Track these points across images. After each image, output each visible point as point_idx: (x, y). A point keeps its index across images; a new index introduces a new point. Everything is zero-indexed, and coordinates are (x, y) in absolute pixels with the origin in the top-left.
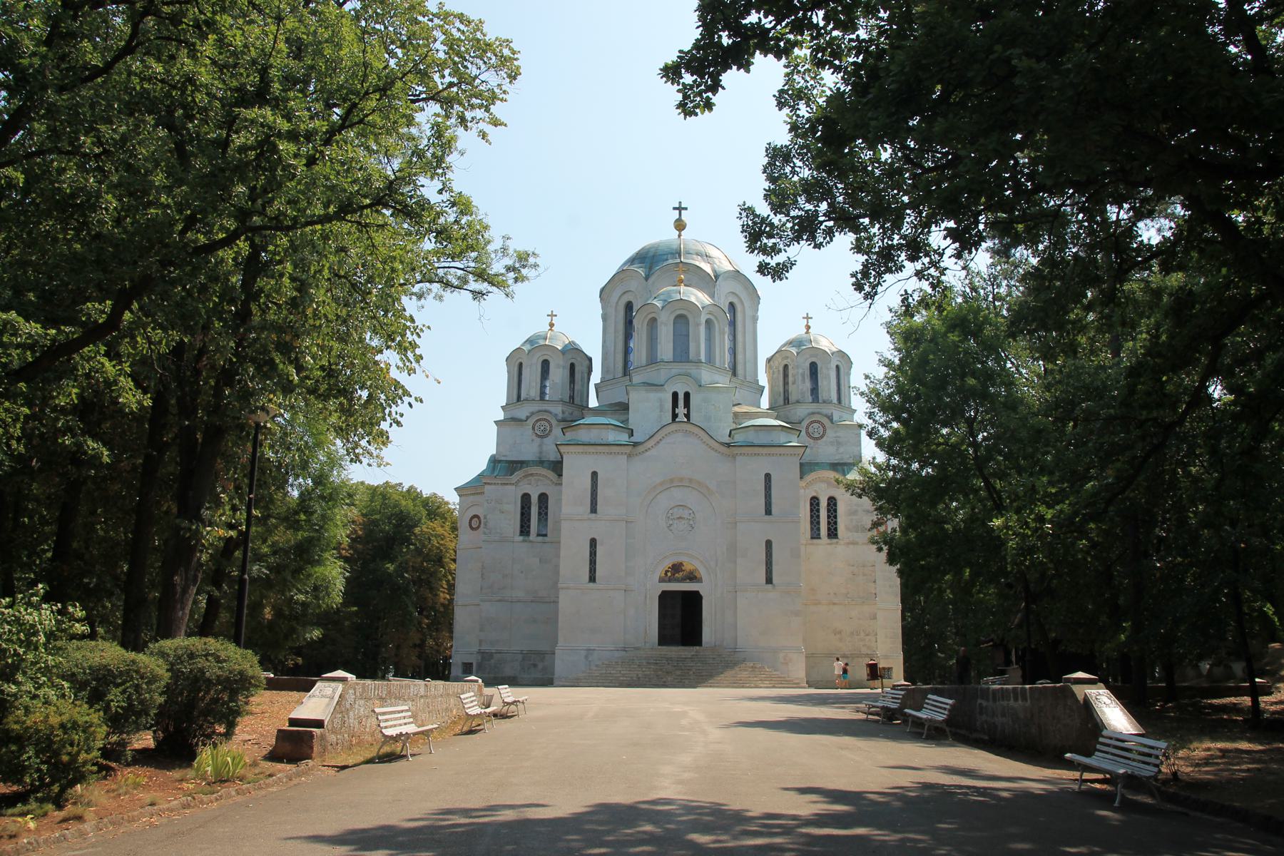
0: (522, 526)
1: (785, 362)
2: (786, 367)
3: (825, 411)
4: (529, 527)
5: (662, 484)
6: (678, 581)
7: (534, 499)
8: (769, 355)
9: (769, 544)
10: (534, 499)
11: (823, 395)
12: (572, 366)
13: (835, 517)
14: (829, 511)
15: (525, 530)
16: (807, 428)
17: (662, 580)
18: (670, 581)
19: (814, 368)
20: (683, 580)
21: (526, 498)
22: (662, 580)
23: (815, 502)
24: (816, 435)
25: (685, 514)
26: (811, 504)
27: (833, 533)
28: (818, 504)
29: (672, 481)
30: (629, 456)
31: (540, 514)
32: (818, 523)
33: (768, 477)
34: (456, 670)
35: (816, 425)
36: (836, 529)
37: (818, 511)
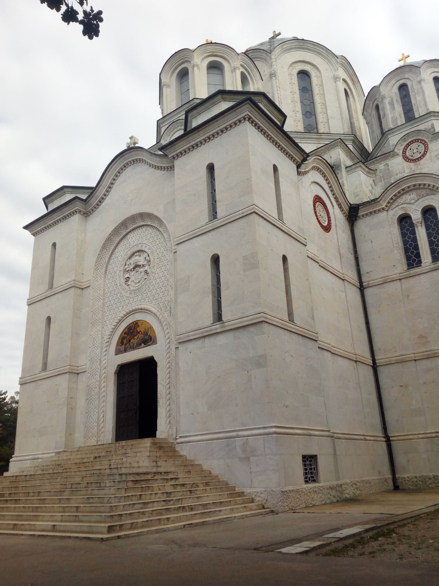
1: (375, 103)
3: (422, 127)
5: (116, 231)
6: (134, 348)
9: (216, 260)
11: (419, 111)
16: (404, 152)
17: (118, 352)
18: (125, 351)
20: (138, 346)
22: (118, 352)
24: (417, 156)
25: (140, 259)
26: (402, 228)
28: (412, 225)
29: (124, 224)
30: (86, 214)
32: (416, 247)
33: (211, 168)
35: (414, 146)
37: (413, 233)
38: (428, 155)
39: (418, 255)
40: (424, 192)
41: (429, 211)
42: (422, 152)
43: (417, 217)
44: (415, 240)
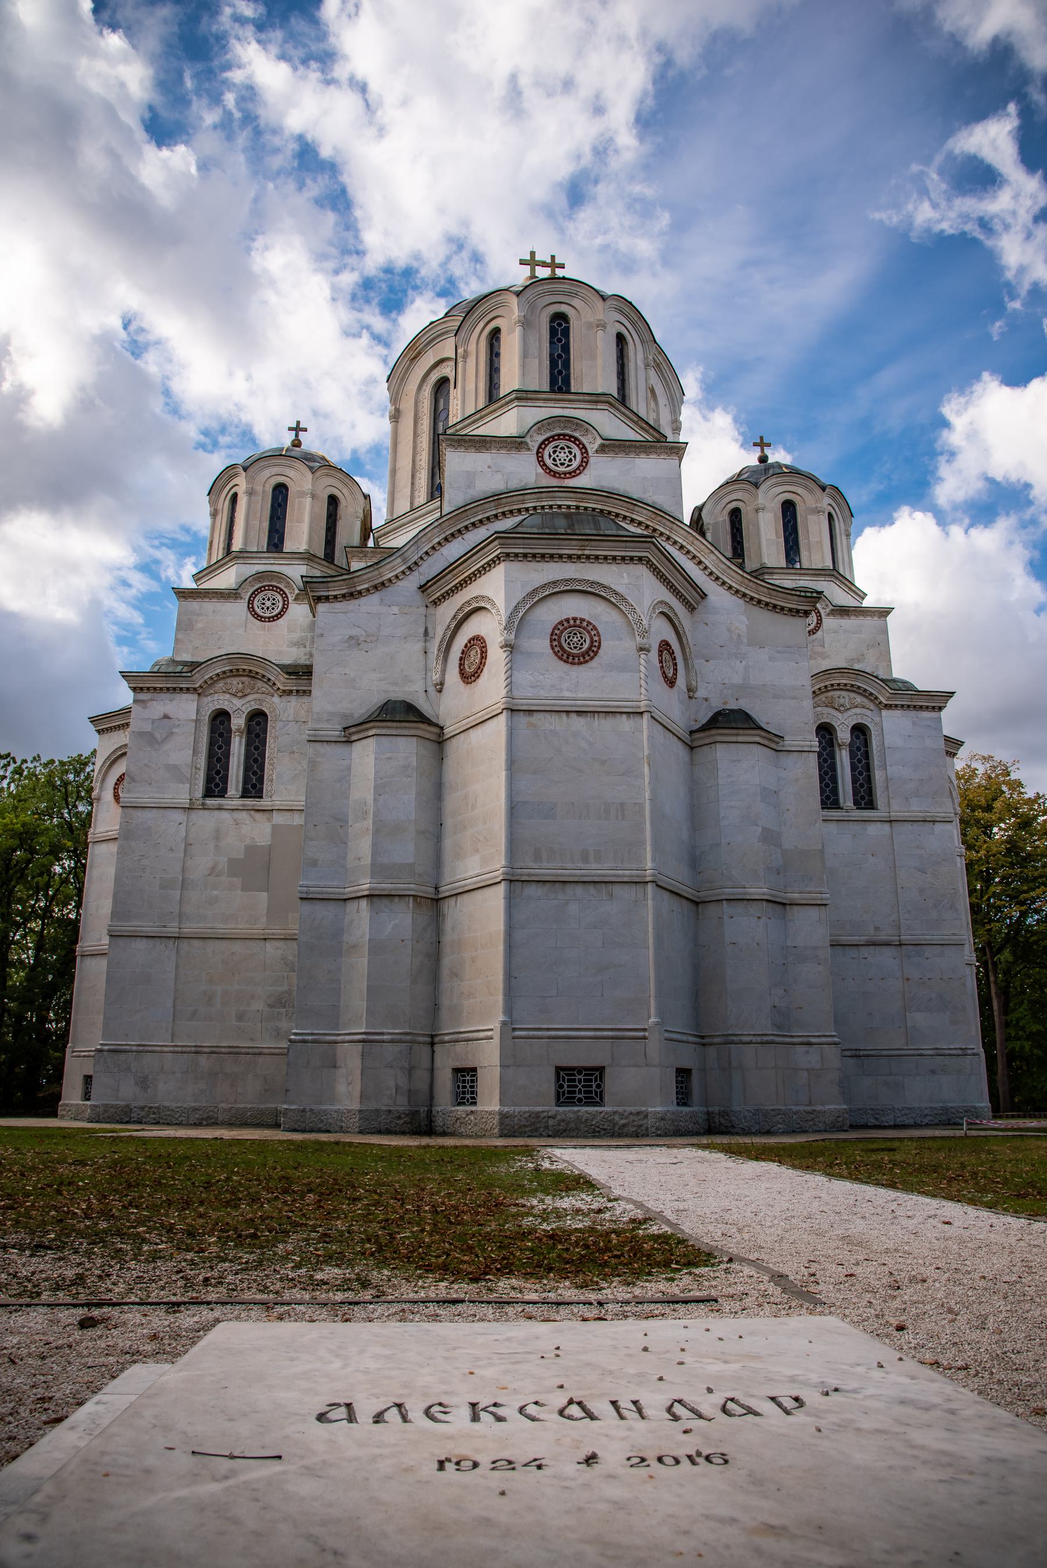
0: (209, 779)
2: (735, 515)
4: (225, 779)
7: (238, 722)
8: (699, 503)
10: (238, 722)
12: (333, 500)
13: (868, 767)
14: (852, 756)
15: (215, 785)
19: (789, 508)
21: (221, 717)
23: (825, 731)
27: (865, 798)
31: (248, 755)
32: (834, 779)
34: (71, 1095)
36: (870, 792)
37: (832, 756)
38: (819, 633)
39: (835, 791)
40: (859, 699)
41: (860, 731)
42: (812, 626)
43: (844, 735)
44: (833, 767)
